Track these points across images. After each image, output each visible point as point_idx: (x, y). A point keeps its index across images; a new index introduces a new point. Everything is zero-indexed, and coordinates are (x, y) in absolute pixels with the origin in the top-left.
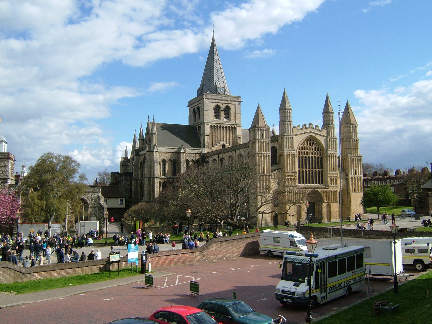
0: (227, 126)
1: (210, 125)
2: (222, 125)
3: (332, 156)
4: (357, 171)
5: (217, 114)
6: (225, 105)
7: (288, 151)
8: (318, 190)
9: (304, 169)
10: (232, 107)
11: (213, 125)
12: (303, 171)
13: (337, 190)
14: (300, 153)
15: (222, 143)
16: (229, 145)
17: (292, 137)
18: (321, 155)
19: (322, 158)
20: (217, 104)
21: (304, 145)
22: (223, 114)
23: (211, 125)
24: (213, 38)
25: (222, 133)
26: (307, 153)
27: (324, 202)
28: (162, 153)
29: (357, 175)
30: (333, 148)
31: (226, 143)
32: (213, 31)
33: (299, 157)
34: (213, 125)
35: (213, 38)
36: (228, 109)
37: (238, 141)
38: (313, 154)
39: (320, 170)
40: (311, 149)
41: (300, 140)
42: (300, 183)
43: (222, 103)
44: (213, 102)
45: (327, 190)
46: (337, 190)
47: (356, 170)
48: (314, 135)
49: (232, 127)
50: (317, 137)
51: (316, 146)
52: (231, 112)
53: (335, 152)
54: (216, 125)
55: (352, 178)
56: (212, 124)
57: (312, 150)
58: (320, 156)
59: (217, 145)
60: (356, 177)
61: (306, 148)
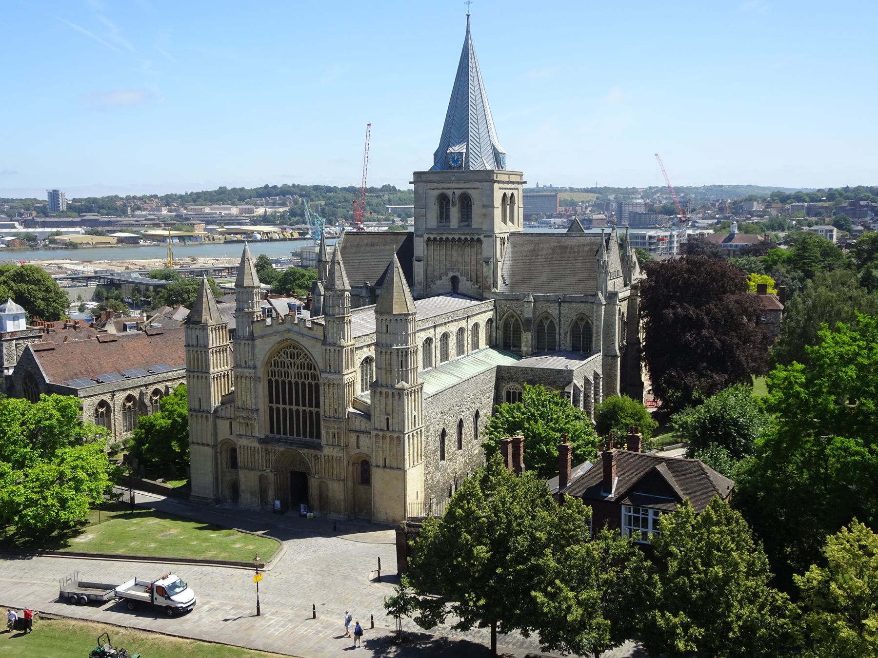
0: (463, 237)
1: (426, 236)
2: (450, 237)
4: (390, 421)
5: (444, 215)
6: (458, 192)
7: (240, 370)
8: (301, 452)
9: (281, 406)
10: (473, 193)
11: (432, 238)
12: (278, 409)
13: (340, 458)
14: (273, 373)
15: (451, 274)
16: (465, 278)
19: (317, 386)
20: (440, 191)
21: (279, 358)
22: (455, 212)
23: (429, 238)
24: (468, 32)
25: (454, 254)
26: (287, 374)
27: (314, 477)
29: (391, 429)
32: (468, 16)
33: (270, 381)
34: (432, 237)
35: (468, 32)
36: (466, 201)
37: (485, 269)
38: (299, 376)
39: (314, 410)
41: (268, 347)
42: (272, 431)
45: (318, 453)
46: (340, 458)
47: (388, 419)
49: (472, 239)
50: (305, 343)
51: (306, 360)
54: (438, 238)
57: (298, 368)
58: (313, 383)
59: (441, 277)
61: (283, 364)
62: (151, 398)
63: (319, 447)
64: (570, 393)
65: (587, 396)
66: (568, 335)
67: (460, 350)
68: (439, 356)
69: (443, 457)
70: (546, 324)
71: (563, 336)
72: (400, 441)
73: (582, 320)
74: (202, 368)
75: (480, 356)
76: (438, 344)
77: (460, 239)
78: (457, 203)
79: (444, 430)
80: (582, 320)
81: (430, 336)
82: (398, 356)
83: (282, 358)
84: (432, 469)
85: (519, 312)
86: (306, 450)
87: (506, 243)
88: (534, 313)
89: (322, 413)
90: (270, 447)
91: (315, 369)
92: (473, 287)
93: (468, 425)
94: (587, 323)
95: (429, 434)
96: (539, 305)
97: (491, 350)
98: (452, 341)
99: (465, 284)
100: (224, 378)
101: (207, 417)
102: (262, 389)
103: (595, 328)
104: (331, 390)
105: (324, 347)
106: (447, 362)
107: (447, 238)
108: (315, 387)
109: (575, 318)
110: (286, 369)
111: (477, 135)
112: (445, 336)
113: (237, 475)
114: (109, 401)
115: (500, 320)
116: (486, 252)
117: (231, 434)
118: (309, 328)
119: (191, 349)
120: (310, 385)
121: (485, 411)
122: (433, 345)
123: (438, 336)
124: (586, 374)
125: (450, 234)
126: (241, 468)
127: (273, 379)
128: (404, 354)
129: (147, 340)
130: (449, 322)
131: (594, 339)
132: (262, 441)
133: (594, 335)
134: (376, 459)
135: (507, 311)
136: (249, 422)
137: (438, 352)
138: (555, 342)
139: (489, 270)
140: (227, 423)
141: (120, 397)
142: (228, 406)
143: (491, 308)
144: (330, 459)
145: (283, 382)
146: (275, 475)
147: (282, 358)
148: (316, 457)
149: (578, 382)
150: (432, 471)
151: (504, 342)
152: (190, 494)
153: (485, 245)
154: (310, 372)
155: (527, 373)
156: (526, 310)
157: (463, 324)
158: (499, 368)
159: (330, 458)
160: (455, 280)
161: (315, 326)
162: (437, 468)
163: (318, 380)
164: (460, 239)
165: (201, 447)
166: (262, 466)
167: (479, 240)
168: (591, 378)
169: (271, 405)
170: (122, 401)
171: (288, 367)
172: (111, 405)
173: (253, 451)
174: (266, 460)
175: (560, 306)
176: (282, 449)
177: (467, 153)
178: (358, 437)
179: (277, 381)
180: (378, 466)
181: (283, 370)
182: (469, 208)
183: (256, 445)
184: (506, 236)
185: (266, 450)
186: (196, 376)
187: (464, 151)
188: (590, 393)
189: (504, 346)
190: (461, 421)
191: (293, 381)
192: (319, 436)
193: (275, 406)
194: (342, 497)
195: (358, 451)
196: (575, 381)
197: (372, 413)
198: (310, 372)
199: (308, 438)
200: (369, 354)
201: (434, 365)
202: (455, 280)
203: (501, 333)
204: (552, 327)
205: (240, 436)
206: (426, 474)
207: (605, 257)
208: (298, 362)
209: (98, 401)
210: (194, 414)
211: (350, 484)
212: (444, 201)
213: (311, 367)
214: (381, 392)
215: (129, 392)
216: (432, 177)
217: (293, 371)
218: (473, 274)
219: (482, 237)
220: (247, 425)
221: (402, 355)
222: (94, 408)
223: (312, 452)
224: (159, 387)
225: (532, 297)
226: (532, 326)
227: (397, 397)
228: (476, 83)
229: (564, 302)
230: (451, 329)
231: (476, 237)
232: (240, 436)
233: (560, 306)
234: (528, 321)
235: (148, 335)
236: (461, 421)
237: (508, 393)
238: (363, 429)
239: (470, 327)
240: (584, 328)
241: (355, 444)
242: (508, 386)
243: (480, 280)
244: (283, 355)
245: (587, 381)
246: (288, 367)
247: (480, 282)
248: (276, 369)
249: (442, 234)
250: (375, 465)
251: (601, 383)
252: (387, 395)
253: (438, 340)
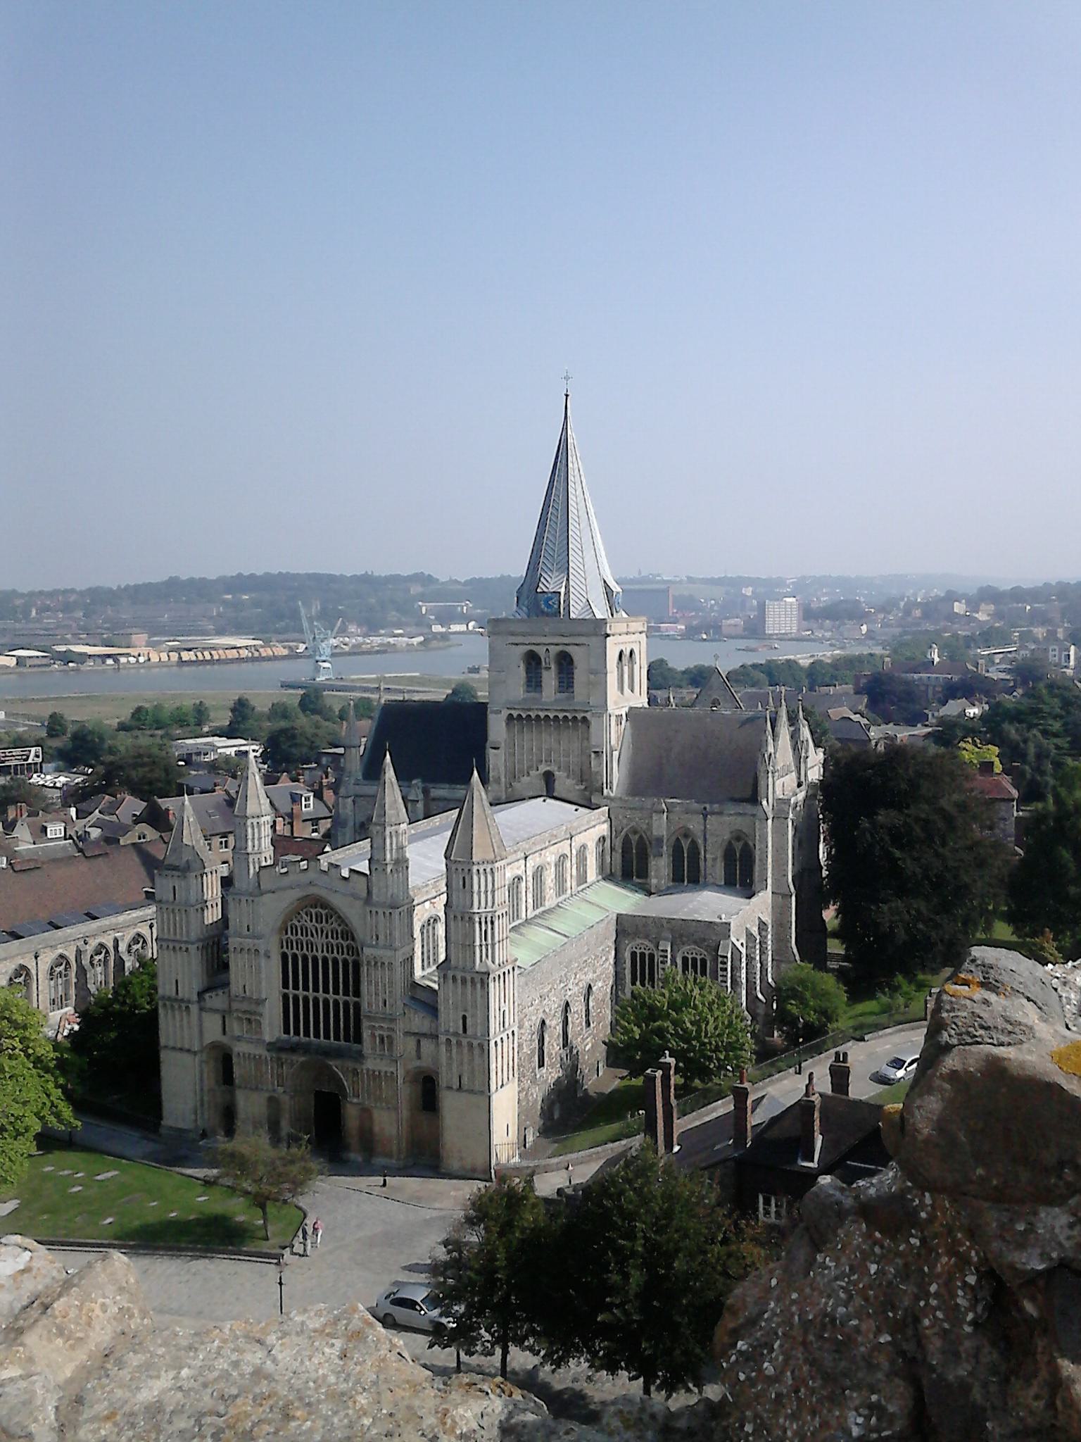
0: (561, 715)
1: (505, 713)
2: (542, 714)
3: (377, 963)
4: (468, 1020)
5: (534, 682)
6: (554, 650)
8: (331, 1063)
11: (515, 716)
14: (289, 943)
15: (543, 768)
16: (566, 774)
17: (250, 899)
18: (355, 953)
19: (357, 966)
21: (299, 921)
22: (550, 679)
23: (510, 716)
25: (548, 739)
26: (311, 945)
28: (368, 799)
29: (469, 1032)
30: (381, 937)
31: (556, 768)
33: (284, 957)
34: (515, 714)
36: (565, 662)
38: (330, 947)
39: (351, 999)
40: (322, 932)
42: (287, 1031)
43: (545, 644)
44: (517, 644)
46: (392, 1073)
47: (464, 1018)
48: (323, 893)
49: (575, 718)
50: (337, 901)
51: (339, 925)
52: (576, 671)
53: (389, 953)
54: (524, 716)
55: (448, 1040)
56: (513, 712)
57: (327, 937)
58: (350, 959)
60: (465, 1042)
61: (305, 931)
62: (92, 957)
63: (360, 1056)
64: (726, 957)
65: (750, 959)
66: (718, 860)
67: (561, 889)
68: (530, 901)
69: (541, 1064)
70: (685, 844)
71: (709, 863)
72: (484, 1050)
73: (738, 839)
74: (181, 934)
75: (590, 895)
76: (530, 884)
77: (556, 717)
78: (553, 666)
79: (543, 1022)
80: (738, 839)
81: (520, 872)
82: (480, 923)
83: (303, 922)
84: (527, 1083)
85: (645, 827)
86: (338, 1062)
87: (623, 722)
88: (668, 828)
89: (365, 1006)
90: (284, 1056)
91: (353, 939)
92: (577, 787)
93: (578, 1007)
94: (746, 844)
95: (522, 1031)
96: (674, 817)
97: (603, 883)
98: (550, 877)
99: (564, 783)
100: (212, 947)
101: (187, 1007)
102: (272, 970)
103: (757, 853)
104: (379, 973)
105: (368, 910)
106: (542, 909)
107: (538, 716)
108: (353, 966)
109: (727, 837)
110: (309, 936)
111: (583, 580)
112: (539, 873)
113: (232, 1094)
114: (31, 965)
115: (616, 837)
116: (593, 741)
117: (224, 1032)
118: (345, 878)
119: (164, 907)
120: (345, 962)
121: (600, 984)
122: (523, 884)
123: (530, 873)
124: (748, 926)
125: (542, 710)
126: (240, 1087)
127: (289, 953)
128: (489, 919)
129: (84, 866)
130: (546, 848)
131: (757, 868)
132: (271, 1047)
133: (757, 861)
134: (446, 1078)
135: (627, 825)
136: (253, 1018)
137: (530, 895)
138: (699, 871)
139: (601, 764)
140: (217, 1019)
141: (47, 959)
142: (220, 992)
143: (604, 819)
144: (375, 1076)
145: (305, 958)
146: (292, 1097)
147: (303, 922)
148: (355, 1073)
149: (737, 939)
150: (527, 1086)
151: (623, 871)
152: (160, 1124)
153: (592, 729)
154: (345, 944)
155: (662, 926)
156: (655, 825)
157: (564, 847)
158: (619, 916)
159: (377, 1073)
160: (549, 778)
161: (355, 876)
162: (534, 1081)
163: (358, 955)
164: (556, 717)
165: (179, 1055)
166: (273, 1084)
167: (584, 718)
168: (755, 931)
169: (286, 991)
170: (47, 967)
171: (312, 936)
172: (33, 972)
173: (258, 1060)
174: (278, 1075)
175: (705, 819)
176: (303, 1059)
177: (567, 592)
178: (419, 1042)
179: (295, 957)
180: (449, 1088)
181: (304, 939)
182: (570, 674)
183: (265, 1053)
184: (623, 712)
185: (279, 1059)
186: (171, 947)
187: (563, 590)
188: (755, 953)
189: (623, 875)
190: (567, 1004)
191: (320, 955)
192: (358, 1039)
193: (291, 992)
194: (394, 1132)
195: (418, 1063)
196: (733, 939)
197: (441, 1008)
198: (345, 944)
199: (343, 1042)
200: (433, 912)
201: (524, 916)
202: (549, 778)
203: (618, 856)
204: (694, 845)
205: (239, 1039)
206: (519, 1092)
207: (771, 749)
208: (327, 927)
209: (14, 967)
210: (168, 1003)
211: (405, 1113)
212: (532, 661)
213: (348, 934)
214: (454, 978)
215: (60, 951)
216: (513, 628)
217: (319, 941)
218: (577, 769)
219: (588, 715)
220: (249, 1021)
221: (486, 922)
222: (8, 978)
223: (350, 1064)
224: (103, 941)
225: (664, 805)
226: (665, 848)
227: (479, 986)
228: (579, 490)
229: (713, 813)
230: (548, 859)
231: (579, 716)
232: (239, 1039)
233: (705, 819)
234: (659, 840)
235: (86, 857)
236: (567, 1004)
237: (633, 954)
238: (425, 1029)
239: (574, 852)
240: (742, 850)
241: (414, 1053)
242: (633, 944)
243: (585, 777)
244: (304, 916)
245: (749, 935)
246: (312, 936)
247: (586, 780)
248: (294, 938)
249: (529, 710)
250: (445, 1085)
251: (769, 937)
252: (464, 981)
253: (530, 879)
